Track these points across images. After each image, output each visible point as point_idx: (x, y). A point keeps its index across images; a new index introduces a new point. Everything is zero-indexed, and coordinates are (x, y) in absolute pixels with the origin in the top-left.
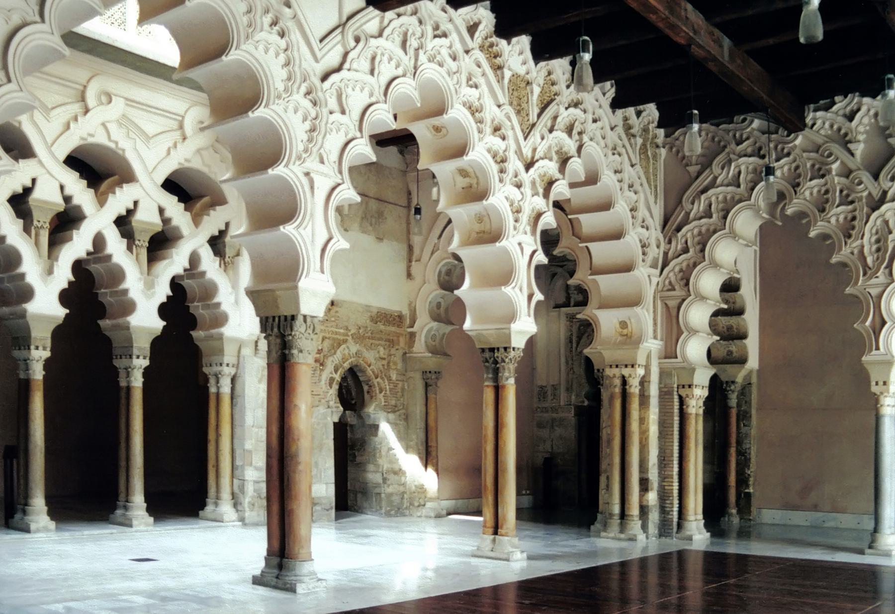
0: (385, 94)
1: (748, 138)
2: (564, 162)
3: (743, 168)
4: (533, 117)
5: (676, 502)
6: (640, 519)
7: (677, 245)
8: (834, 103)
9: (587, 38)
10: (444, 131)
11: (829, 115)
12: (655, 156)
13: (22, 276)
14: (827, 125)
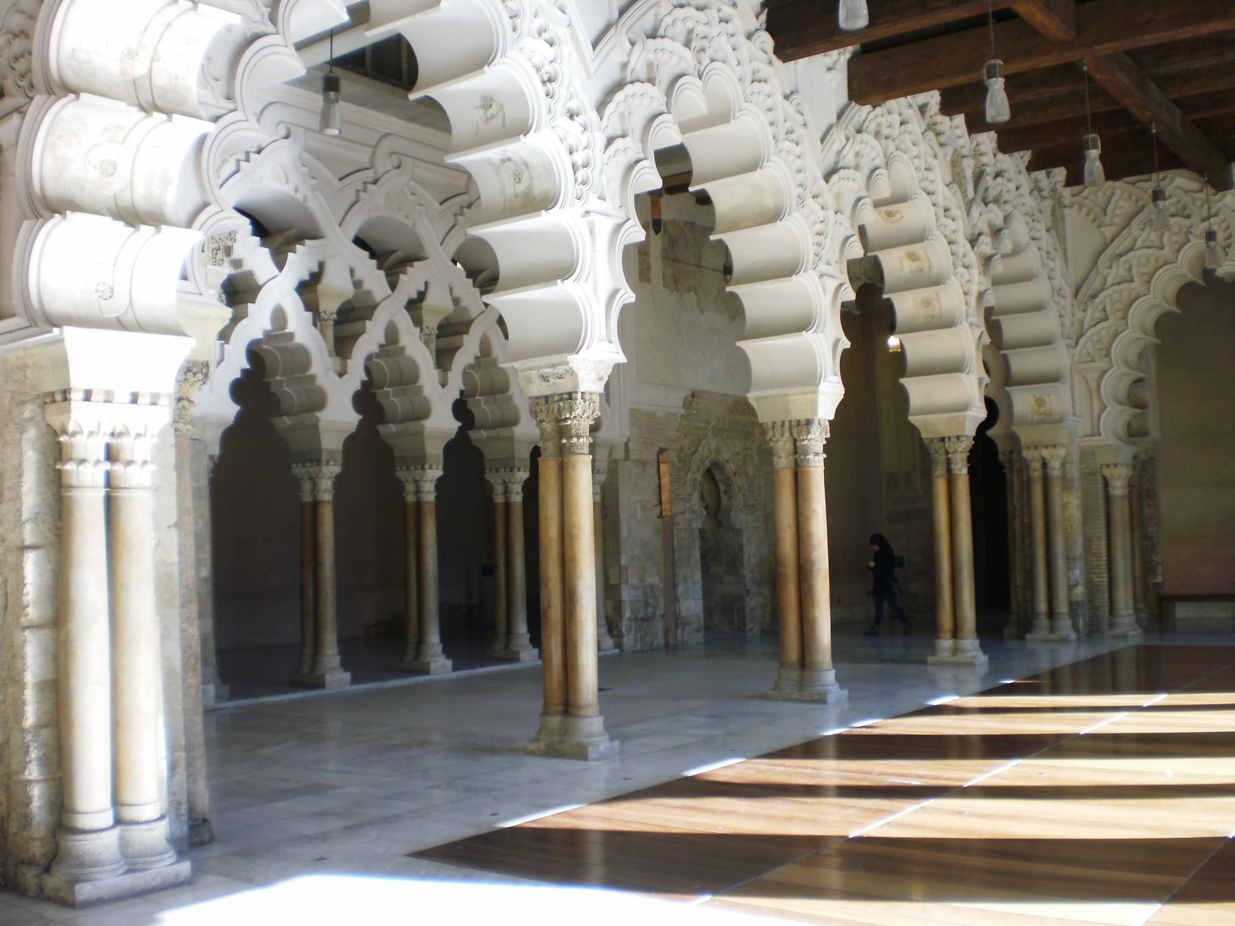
2: (996, 233)
4: (970, 193)
5: (1106, 596)
7: (1093, 313)
9: (1093, 135)
10: (898, 216)
12: (1063, 217)
13: (313, 378)
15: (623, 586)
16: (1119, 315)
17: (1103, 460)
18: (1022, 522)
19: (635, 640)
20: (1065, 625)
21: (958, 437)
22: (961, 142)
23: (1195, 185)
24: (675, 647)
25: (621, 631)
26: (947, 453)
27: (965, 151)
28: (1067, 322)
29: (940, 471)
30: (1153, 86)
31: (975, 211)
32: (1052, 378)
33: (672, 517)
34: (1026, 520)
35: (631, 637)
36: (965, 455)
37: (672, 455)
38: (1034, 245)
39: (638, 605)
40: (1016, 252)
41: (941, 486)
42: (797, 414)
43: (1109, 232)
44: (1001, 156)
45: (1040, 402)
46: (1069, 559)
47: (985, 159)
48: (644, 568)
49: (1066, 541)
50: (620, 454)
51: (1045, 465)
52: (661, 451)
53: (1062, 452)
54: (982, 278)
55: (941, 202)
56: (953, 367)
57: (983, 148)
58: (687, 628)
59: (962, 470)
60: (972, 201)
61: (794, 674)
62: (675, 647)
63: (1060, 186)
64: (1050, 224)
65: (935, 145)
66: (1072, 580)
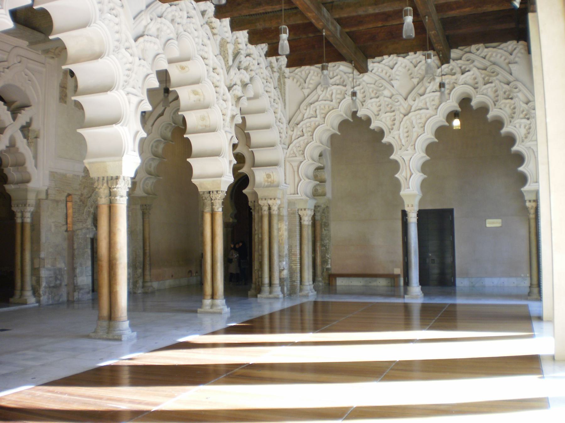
0: (164, 49)
1: (337, 75)
2: (245, 85)
3: (334, 91)
4: (230, 62)
5: (299, 275)
6: (280, 286)
7: (297, 132)
8: (384, 59)
9: (284, 26)
10: (187, 69)
11: (380, 65)
12: (284, 83)
14: (380, 70)
15: (41, 269)
16: (310, 134)
17: (298, 206)
18: (258, 237)
19: (48, 299)
20: (277, 289)
21: (217, 192)
22: (227, 35)
23: (350, 70)
24: (73, 302)
25: (39, 294)
26: (212, 200)
27: (229, 40)
28: (283, 135)
29: (208, 209)
30: (325, 10)
31: (233, 71)
32: (275, 164)
33: (73, 231)
34: (260, 236)
35: (46, 297)
36: (221, 201)
37: (76, 198)
38: (267, 95)
39: (51, 279)
40: (256, 97)
41: (208, 217)
42: (112, 173)
43: (306, 92)
44: (250, 46)
45: (269, 176)
46: (280, 256)
47: (240, 46)
48: (55, 259)
49: (279, 247)
50: (43, 196)
51: (270, 209)
52: (69, 195)
53: (278, 202)
54: (234, 107)
55: (210, 62)
56: (216, 154)
57: (240, 40)
58: (82, 291)
59: (219, 209)
60: (231, 67)
61: (105, 324)
62: (73, 302)
63: (284, 67)
64: (276, 85)
65: (210, 35)
66: (282, 267)
